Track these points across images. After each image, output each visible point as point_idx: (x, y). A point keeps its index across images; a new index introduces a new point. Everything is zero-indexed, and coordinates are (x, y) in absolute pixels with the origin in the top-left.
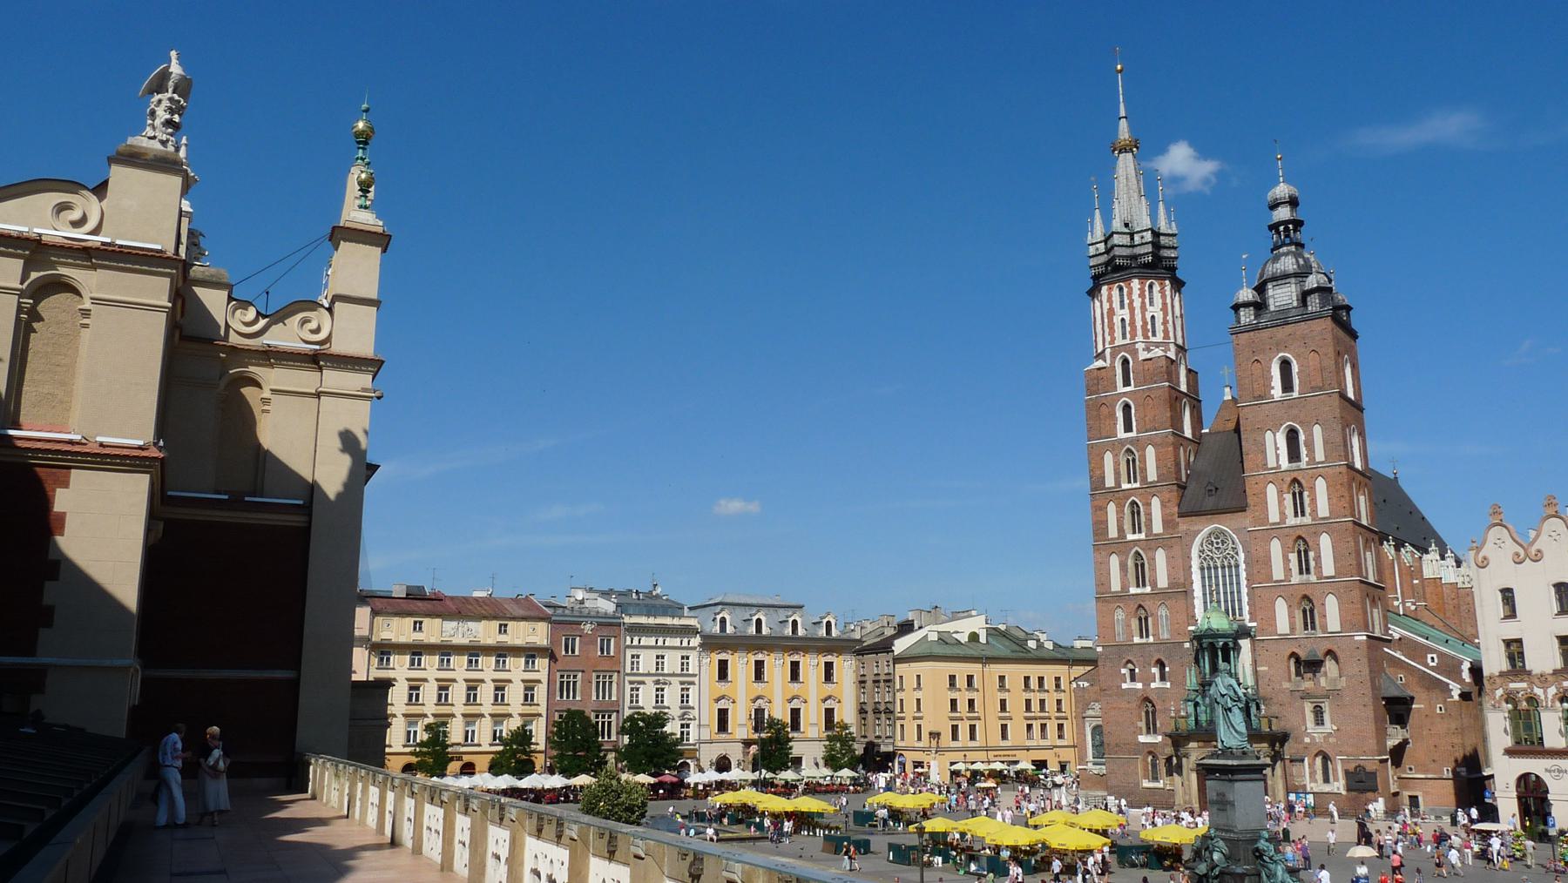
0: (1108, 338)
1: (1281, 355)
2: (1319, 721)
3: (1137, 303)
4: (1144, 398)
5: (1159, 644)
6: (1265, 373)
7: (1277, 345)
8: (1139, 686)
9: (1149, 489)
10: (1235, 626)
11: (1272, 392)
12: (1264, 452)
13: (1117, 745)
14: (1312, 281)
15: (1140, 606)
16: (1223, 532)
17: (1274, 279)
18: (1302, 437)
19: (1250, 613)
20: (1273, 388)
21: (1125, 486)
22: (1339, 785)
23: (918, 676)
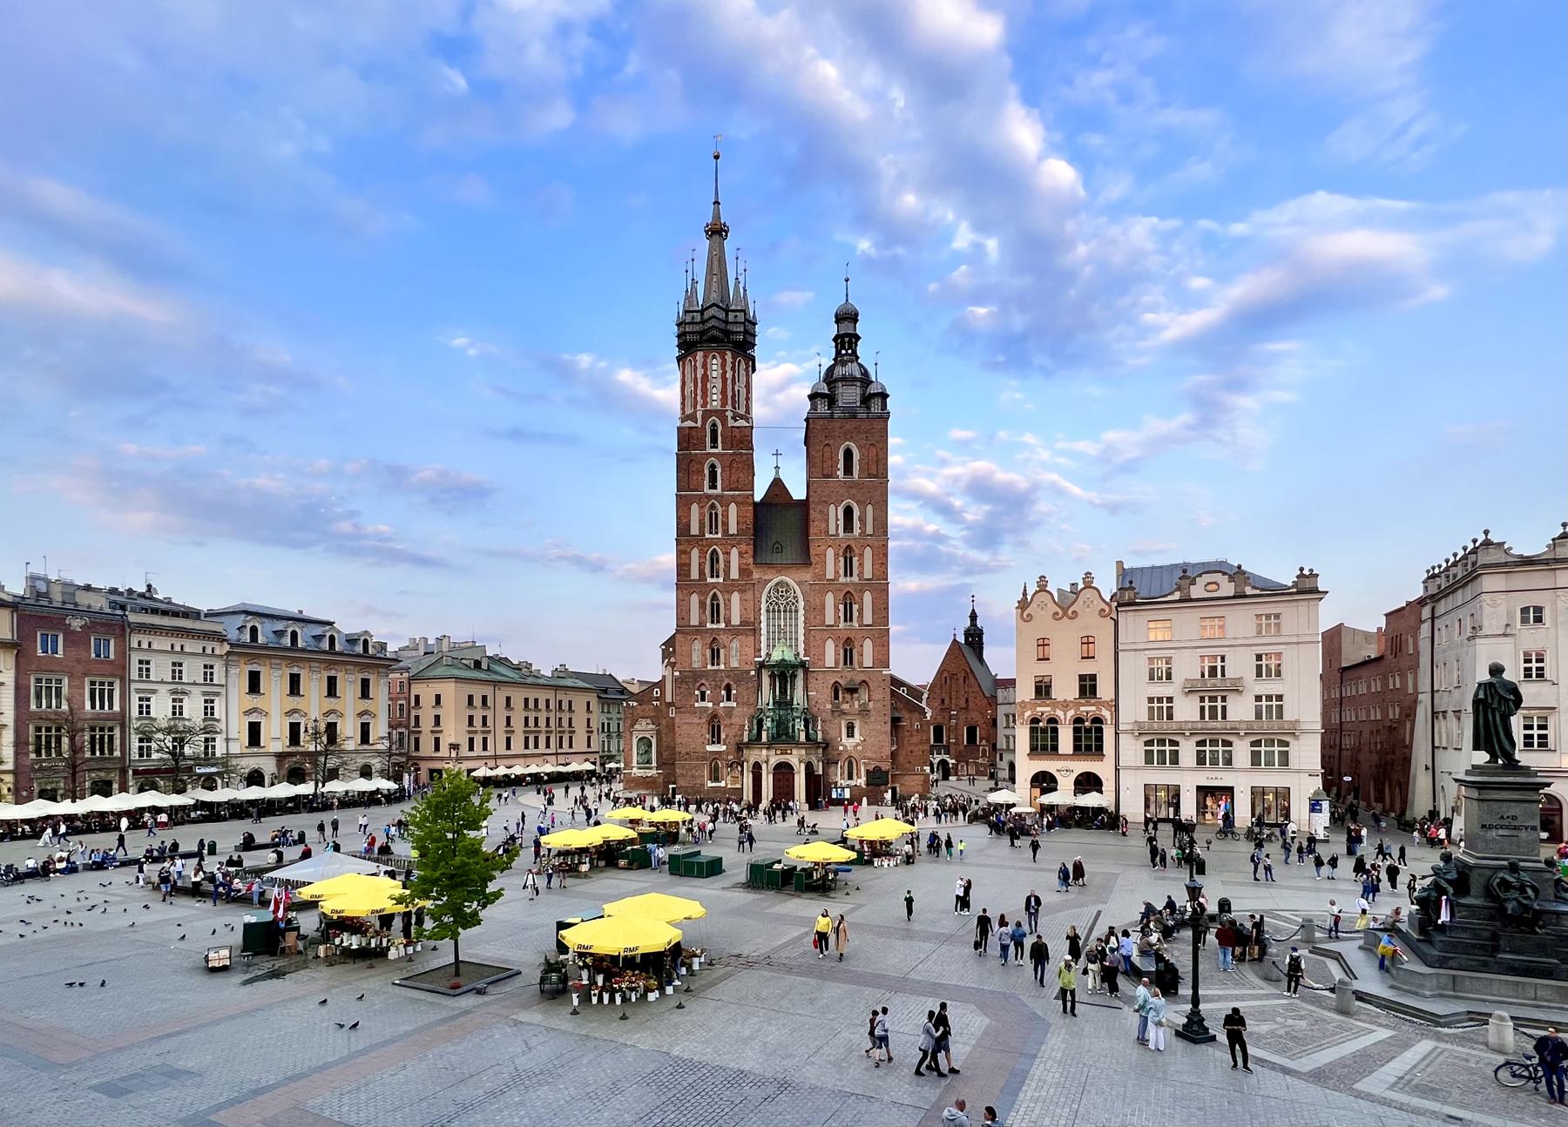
5: (731, 672)
7: (845, 434)
8: (710, 705)
12: (827, 521)
13: (687, 753)
15: (715, 639)
16: (787, 585)
17: (844, 379)
19: (805, 650)
21: (708, 536)
22: (861, 781)
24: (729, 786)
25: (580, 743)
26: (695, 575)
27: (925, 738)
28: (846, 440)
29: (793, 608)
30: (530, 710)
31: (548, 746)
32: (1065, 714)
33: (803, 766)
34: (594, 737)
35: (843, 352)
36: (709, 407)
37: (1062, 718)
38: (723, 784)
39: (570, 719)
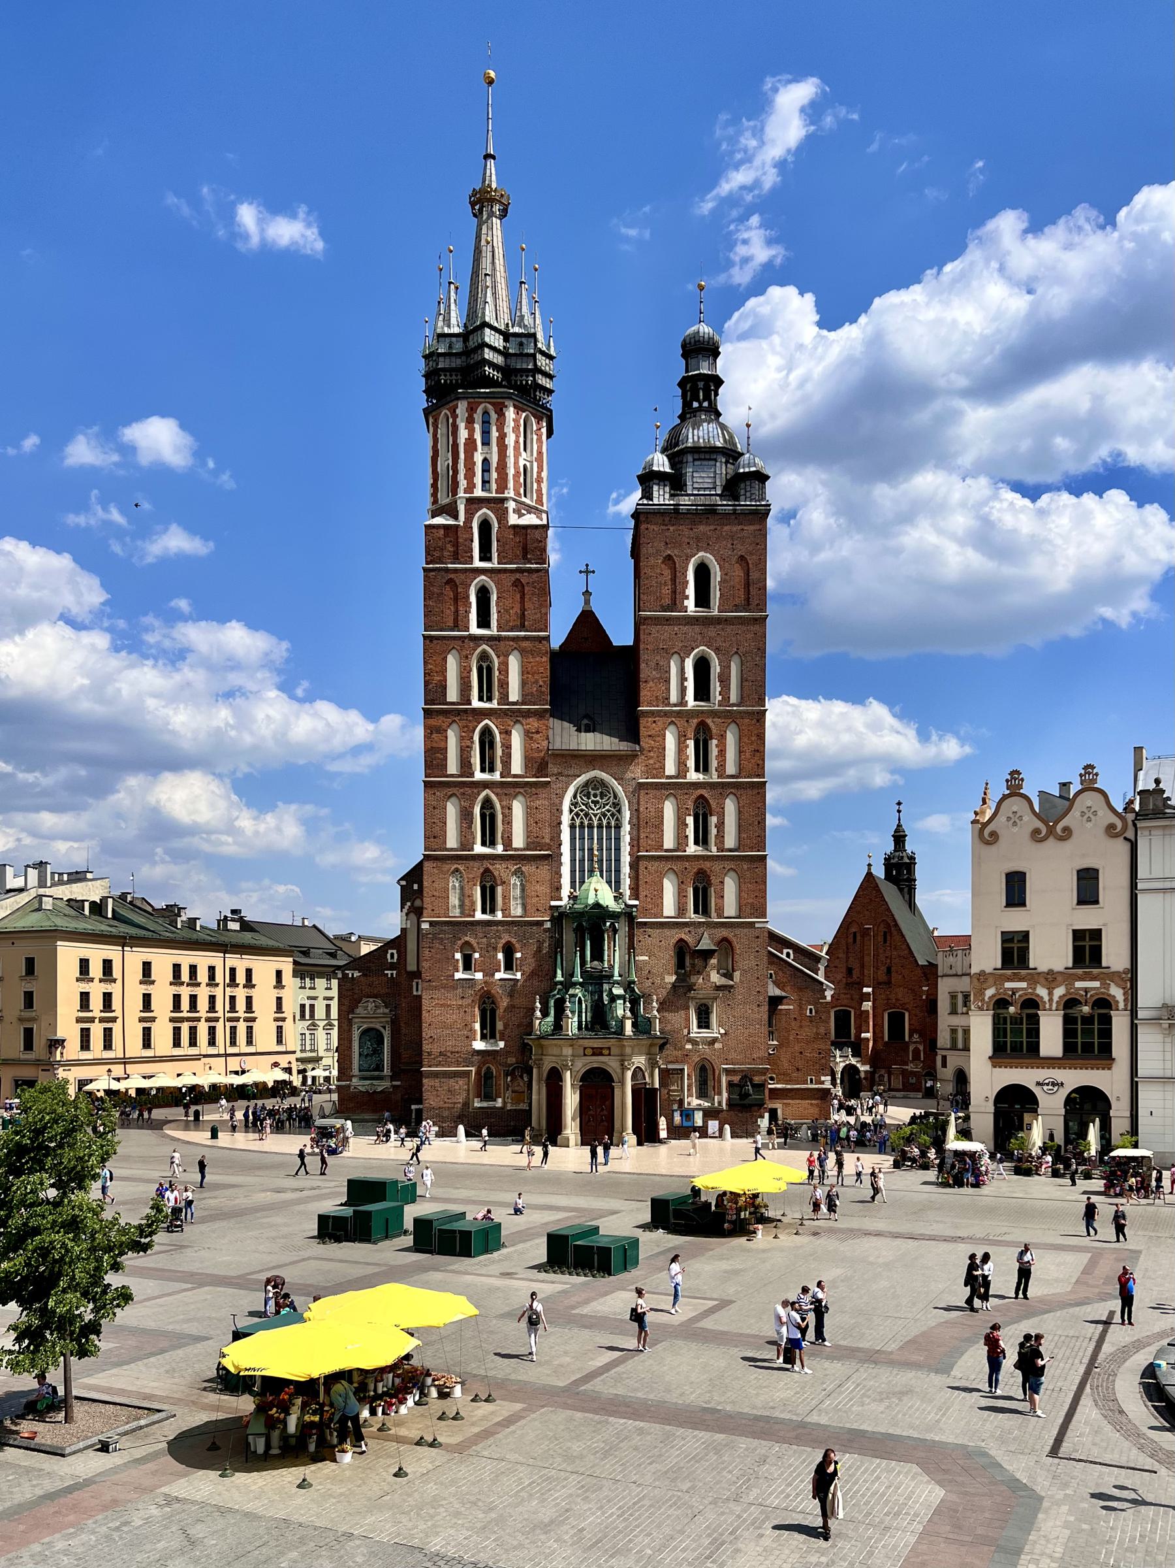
0: (463, 483)
1: (701, 554)
2: (704, 1023)
6: (678, 574)
8: (479, 976)
12: (668, 681)
15: (487, 870)
16: (602, 783)
18: (716, 668)
20: (687, 598)
21: (476, 703)
24: (509, 1107)
25: (265, 1037)
26: (453, 767)
27: (822, 1030)
28: (698, 551)
30: (182, 983)
31: (212, 1042)
32: (1050, 994)
33: (629, 1074)
34: (288, 1026)
35: (695, 405)
37: (1046, 998)
38: (499, 1103)
39: (249, 1000)
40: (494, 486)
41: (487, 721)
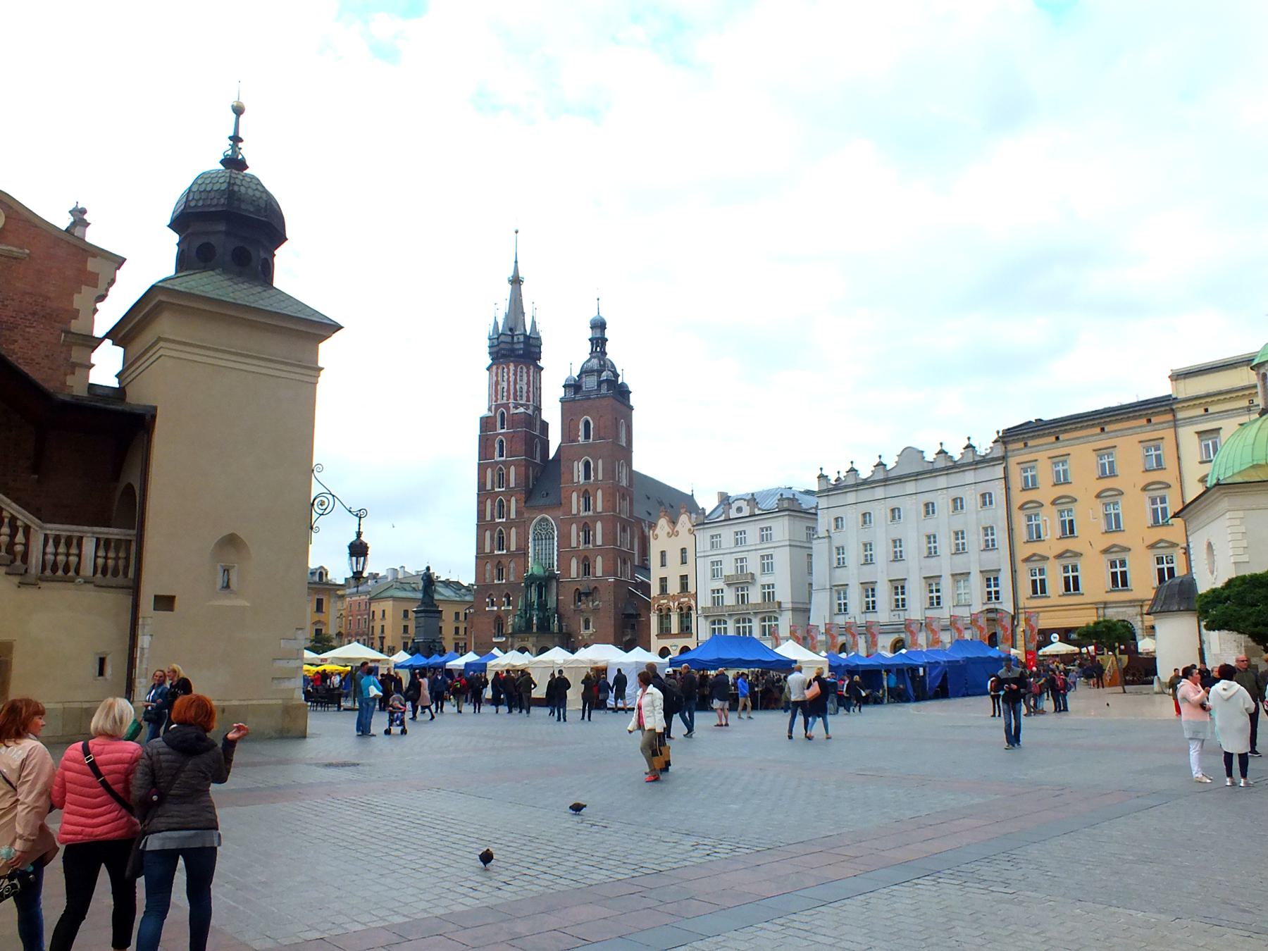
3: (512, 379)
4: (510, 438)
5: (509, 584)
8: (495, 608)
9: (510, 492)
10: (547, 574)
11: (579, 438)
14: (604, 376)
15: (499, 562)
16: (547, 520)
19: (557, 566)
21: (497, 490)
23: (384, 611)
26: (488, 518)
29: (551, 537)
36: (499, 402)
40: (505, 398)
41: (501, 497)
